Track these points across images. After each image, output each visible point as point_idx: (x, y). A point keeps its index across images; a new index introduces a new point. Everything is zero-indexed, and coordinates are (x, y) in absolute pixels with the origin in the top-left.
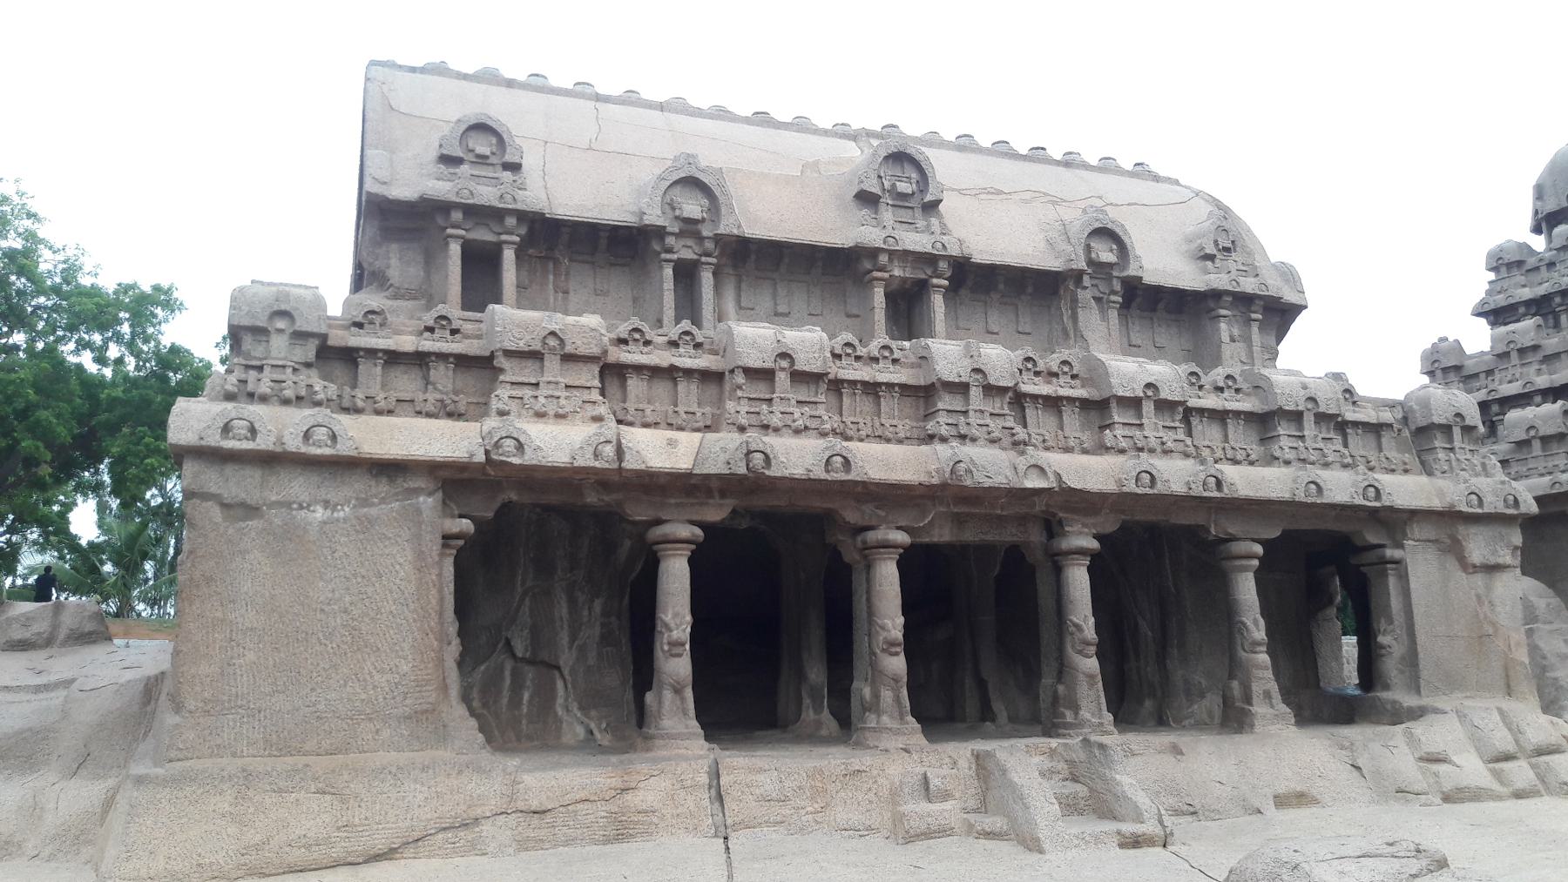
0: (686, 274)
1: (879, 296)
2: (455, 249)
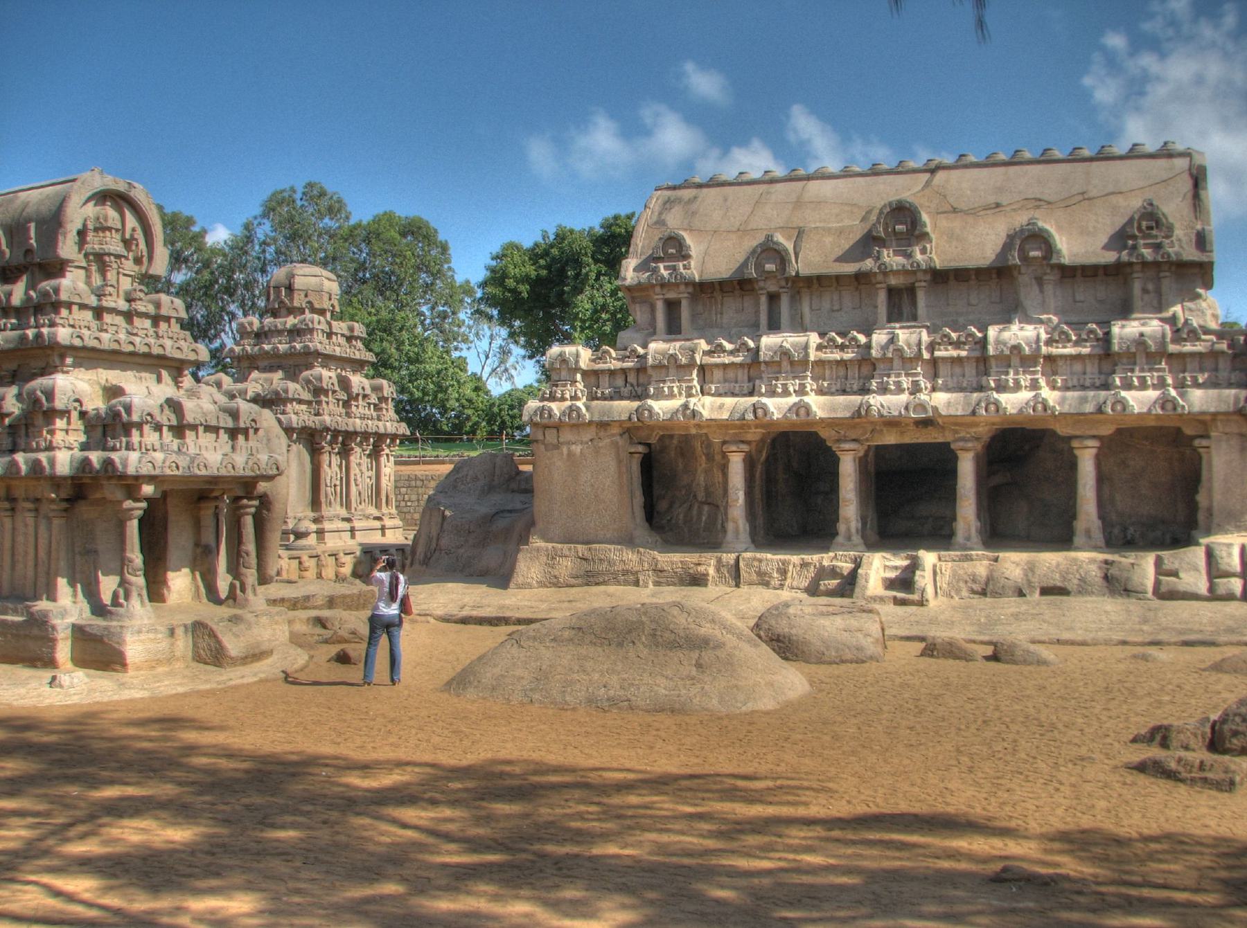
0: (773, 298)
1: (882, 297)
2: (660, 306)
